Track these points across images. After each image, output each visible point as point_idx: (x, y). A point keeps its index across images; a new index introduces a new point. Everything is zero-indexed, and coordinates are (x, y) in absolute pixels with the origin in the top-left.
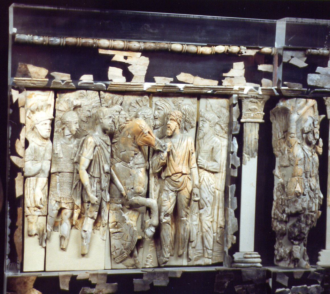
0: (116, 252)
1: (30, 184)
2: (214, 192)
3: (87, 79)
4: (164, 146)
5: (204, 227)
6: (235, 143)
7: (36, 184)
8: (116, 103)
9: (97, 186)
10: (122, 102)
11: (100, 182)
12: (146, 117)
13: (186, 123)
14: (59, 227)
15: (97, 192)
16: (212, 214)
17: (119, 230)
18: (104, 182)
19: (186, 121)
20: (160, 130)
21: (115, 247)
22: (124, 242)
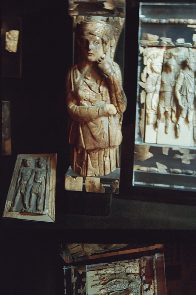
3: (144, 278)
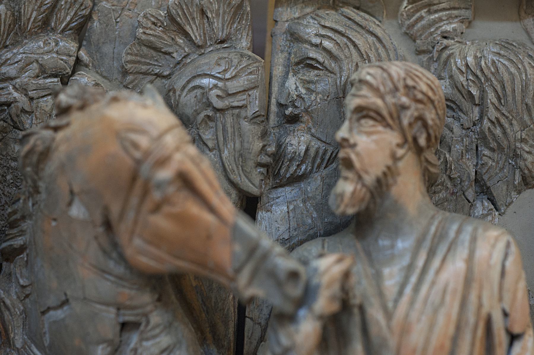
4: (294, 275)
8: (45, 25)
10: (89, 18)
12: (219, 104)
13: (486, 152)
19: (483, 137)
20: (313, 185)
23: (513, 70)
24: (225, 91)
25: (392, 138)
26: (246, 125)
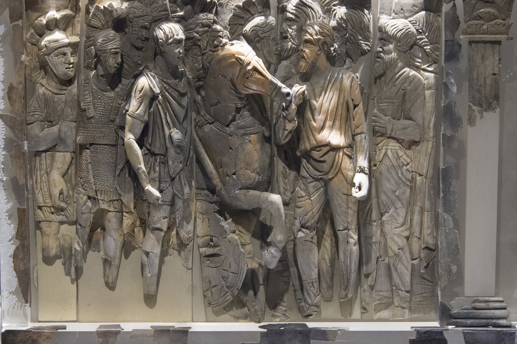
0: (211, 291)
1: (41, 164)
2: (413, 180)
5: (391, 248)
6: (451, 83)
7: (52, 163)
9: (160, 169)
11: (165, 163)
12: (262, 36)
14: (101, 242)
15: (159, 181)
16: (408, 223)
17: (216, 250)
18: (173, 163)
21: (210, 282)
22: (225, 274)
23: (357, 17)
24: (263, 31)
25: (316, 48)
26: (270, 42)
